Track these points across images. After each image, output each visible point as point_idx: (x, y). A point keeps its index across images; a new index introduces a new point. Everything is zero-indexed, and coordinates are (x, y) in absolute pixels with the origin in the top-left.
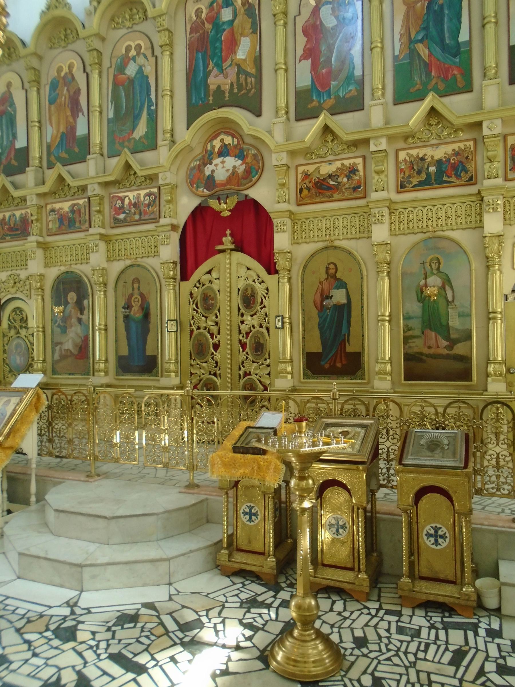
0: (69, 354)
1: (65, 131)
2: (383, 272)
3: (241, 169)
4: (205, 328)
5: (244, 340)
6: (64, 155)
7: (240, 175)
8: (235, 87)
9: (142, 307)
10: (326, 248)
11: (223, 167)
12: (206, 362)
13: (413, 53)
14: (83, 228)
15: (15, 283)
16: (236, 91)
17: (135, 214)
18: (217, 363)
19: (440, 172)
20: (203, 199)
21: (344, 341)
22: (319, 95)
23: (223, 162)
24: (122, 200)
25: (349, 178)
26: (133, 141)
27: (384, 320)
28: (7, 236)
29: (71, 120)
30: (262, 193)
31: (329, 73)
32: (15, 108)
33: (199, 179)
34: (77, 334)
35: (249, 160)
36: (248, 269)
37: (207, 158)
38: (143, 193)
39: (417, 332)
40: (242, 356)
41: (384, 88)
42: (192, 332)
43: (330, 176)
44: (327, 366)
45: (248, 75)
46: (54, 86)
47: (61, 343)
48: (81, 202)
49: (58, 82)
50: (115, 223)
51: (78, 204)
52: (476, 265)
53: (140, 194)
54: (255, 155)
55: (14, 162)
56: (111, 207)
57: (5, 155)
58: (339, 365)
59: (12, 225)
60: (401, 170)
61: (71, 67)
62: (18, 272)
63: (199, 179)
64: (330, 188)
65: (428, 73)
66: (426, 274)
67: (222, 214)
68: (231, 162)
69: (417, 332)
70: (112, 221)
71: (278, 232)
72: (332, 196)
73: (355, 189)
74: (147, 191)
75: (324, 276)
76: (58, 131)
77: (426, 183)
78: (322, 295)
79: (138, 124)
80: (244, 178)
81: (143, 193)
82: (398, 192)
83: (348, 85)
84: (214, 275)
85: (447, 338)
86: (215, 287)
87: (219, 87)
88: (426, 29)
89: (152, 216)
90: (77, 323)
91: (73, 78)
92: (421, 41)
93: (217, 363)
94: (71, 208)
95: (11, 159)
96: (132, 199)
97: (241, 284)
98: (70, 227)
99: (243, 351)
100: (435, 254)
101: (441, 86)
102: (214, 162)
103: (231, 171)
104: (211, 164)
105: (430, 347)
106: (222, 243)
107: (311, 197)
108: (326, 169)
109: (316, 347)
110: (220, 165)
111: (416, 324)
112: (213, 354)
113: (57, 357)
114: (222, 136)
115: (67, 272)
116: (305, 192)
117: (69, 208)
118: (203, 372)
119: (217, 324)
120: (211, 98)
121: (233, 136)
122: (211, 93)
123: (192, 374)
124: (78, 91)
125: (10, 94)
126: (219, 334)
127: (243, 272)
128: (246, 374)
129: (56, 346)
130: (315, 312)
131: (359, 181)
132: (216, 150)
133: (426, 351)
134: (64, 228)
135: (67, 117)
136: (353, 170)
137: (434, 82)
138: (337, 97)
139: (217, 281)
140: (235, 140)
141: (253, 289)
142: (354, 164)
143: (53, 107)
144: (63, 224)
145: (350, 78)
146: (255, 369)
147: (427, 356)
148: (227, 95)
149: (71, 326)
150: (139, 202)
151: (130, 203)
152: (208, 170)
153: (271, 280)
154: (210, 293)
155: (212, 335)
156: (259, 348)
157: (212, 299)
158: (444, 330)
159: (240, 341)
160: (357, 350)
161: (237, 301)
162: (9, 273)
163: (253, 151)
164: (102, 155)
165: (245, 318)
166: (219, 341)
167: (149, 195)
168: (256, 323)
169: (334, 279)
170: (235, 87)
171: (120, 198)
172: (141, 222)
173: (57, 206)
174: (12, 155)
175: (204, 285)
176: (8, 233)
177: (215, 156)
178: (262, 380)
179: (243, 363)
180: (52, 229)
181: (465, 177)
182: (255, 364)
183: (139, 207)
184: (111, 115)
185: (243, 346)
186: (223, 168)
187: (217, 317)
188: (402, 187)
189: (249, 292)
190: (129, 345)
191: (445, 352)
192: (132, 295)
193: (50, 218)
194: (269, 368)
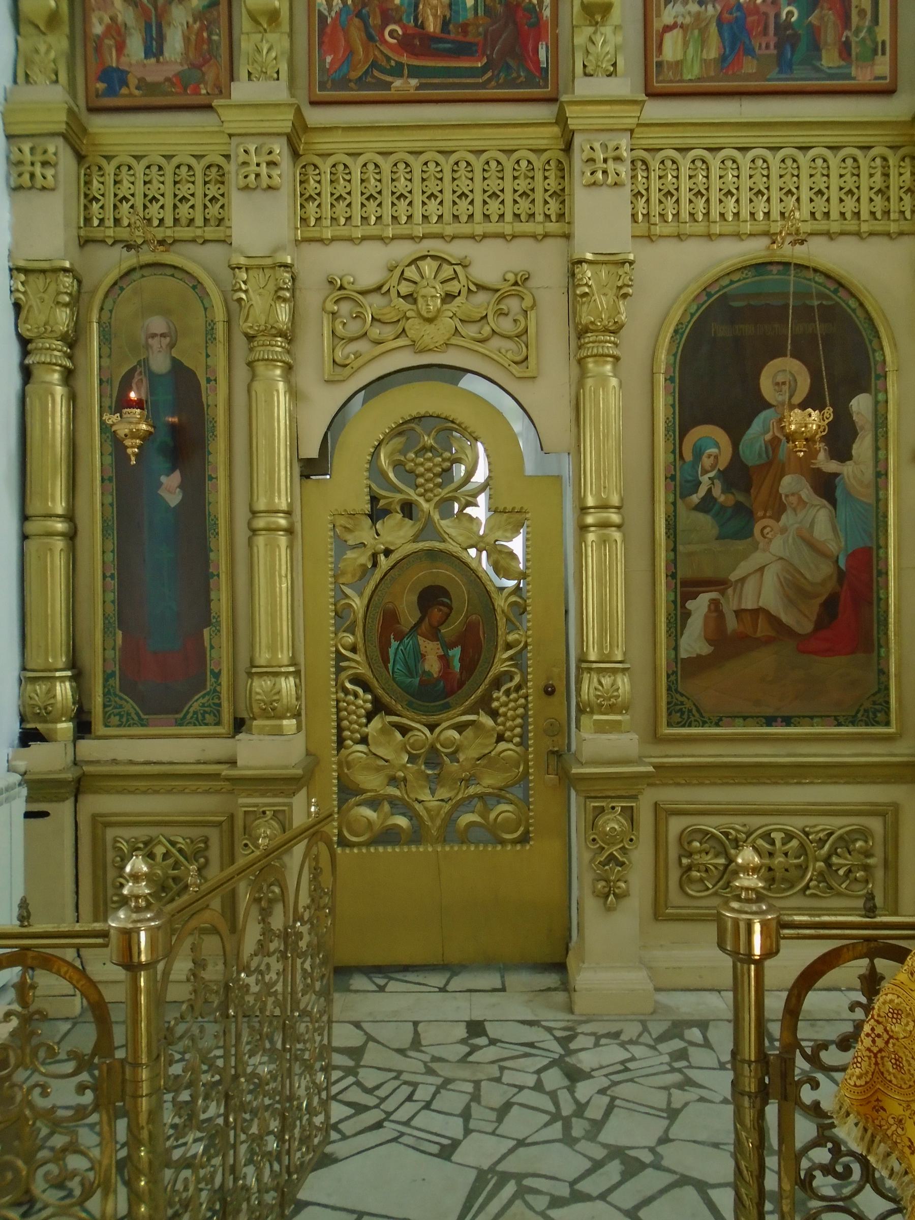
0: (763, 629)
14: (863, 76)
15: (449, 297)
28: (398, 71)
47: (719, 584)
59: (432, 26)
62: (455, 250)
90: (806, 492)
98: (783, 64)
113: (694, 642)
115: (760, 267)
129: (694, 596)
134: (749, 66)
144: (749, 51)
149: (778, 508)
162: (404, 251)
176: (404, 59)
180: (678, 65)
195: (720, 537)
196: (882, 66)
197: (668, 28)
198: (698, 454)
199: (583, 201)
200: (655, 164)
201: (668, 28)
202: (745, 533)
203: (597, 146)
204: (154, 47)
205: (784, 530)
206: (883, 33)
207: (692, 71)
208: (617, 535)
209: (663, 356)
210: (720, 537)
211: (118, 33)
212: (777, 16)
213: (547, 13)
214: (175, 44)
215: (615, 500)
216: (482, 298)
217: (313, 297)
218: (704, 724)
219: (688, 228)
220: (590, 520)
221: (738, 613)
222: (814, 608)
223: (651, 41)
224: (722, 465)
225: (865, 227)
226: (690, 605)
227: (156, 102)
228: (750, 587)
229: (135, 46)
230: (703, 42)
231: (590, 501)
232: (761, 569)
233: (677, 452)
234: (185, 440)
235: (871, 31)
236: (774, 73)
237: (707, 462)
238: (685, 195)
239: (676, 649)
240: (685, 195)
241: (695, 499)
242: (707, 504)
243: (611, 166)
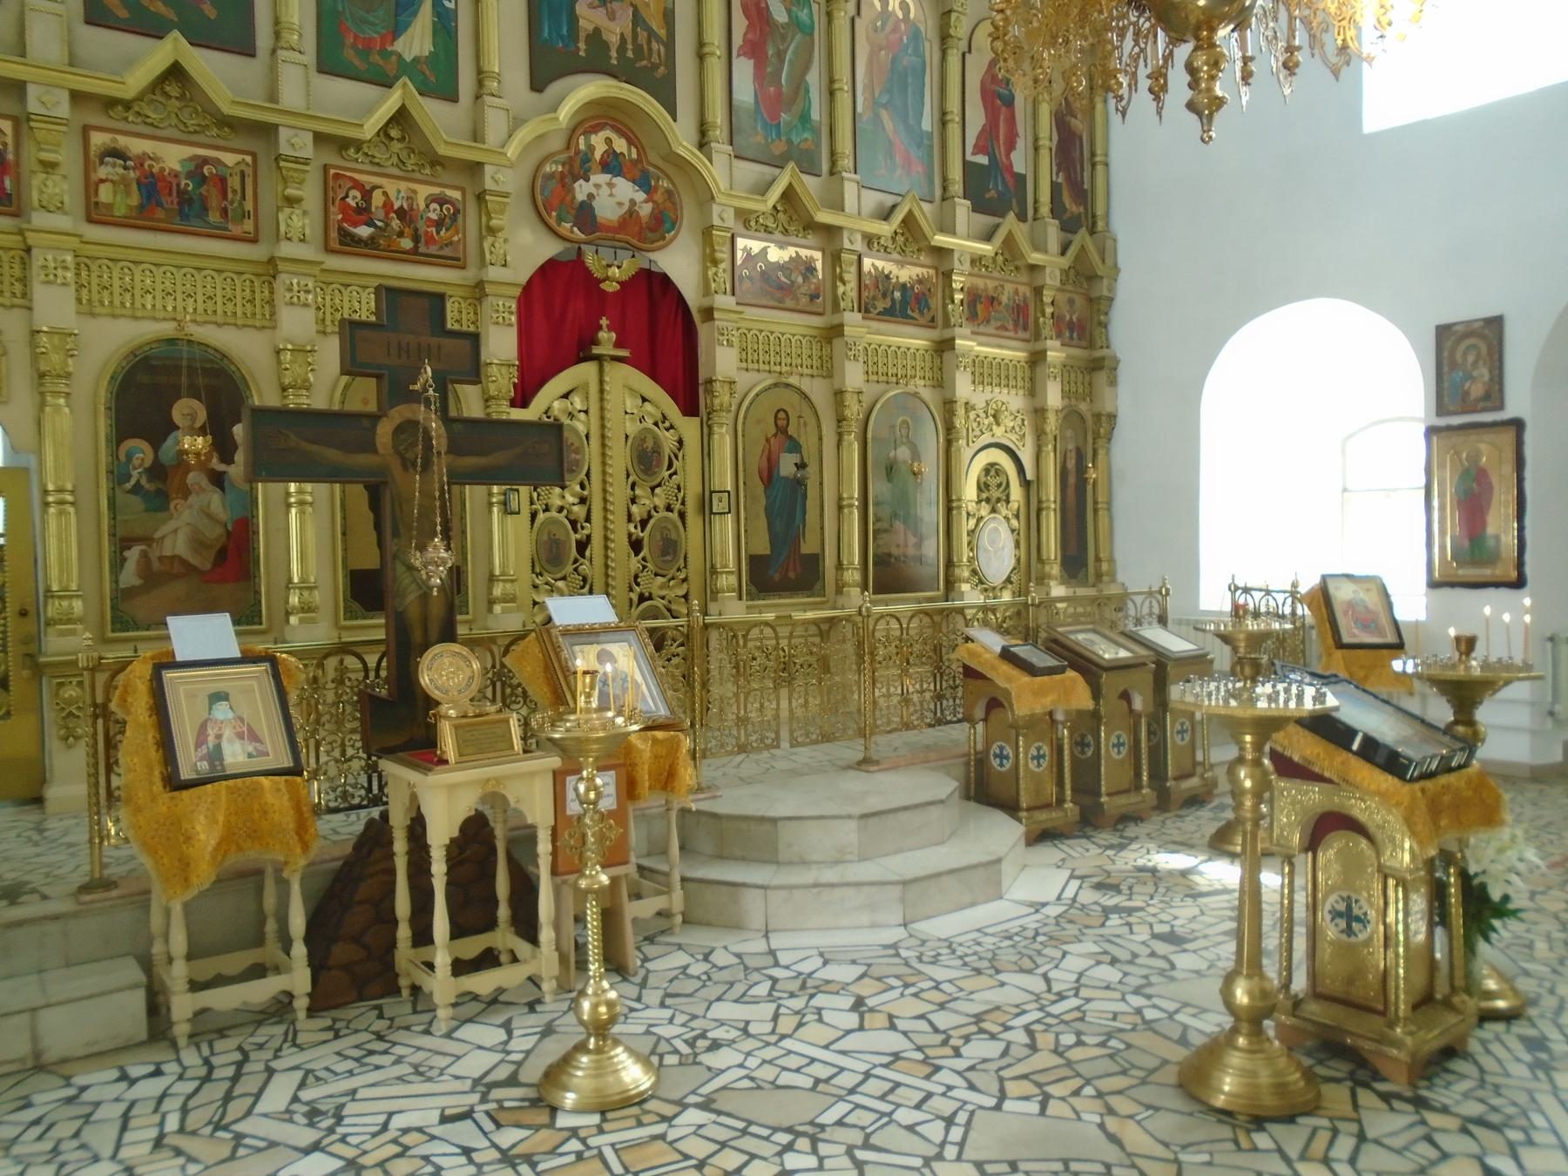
2: (850, 433)
3: (645, 210)
4: (561, 509)
5: (638, 533)
7: (644, 220)
8: (630, 46)
11: (611, 195)
12: (564, 578)
14: (236, 230)
16: (630, 54)
17: (401, 234)
18: (585, 580)
19: (904, 302)
20: (568, 245)
24: (367, 195)
25: (805, 278)
26: (394, 58)
27: (851, 506)
30: (678, 262)
31: (779, 93)
33: (553, 198)
34: (210, 516)
35: (659, 197)
36: (644, 400)
37: (579, 166)
38: (424, 191)
39: (885, 525)
40: (635, 563)
42: (534, 516)
44: (777, 577)
45: (652, 34)
48: (230, 159)
50: (341, 243)
51: (218, 162)
53: (415, 192)
54: (669, 193)
58: (792, 575)
63: (562, 201)
67: (603, 286)
68: (625, 190)
70: (334, 234)
74: (436, 190)
75: (773, 430)
77: (890, 314)
79: (407, 26)
81: (424, 191)
84: (577, 402)
86: (581, 428)
87: (597, 31)
89: (447, 252)
90: (205, 482)
92: (885, 106)
94: (192, 166)
96: (393, 197)
97: (632, 428)
98: (184, 216)
99: (636, 554)
103: (626, 208)
104: (587, 180)
106: (596, 342)
109: (762, 546)
110: (605, 190)
113: (129, 576)
114: (607, 133)
115: (171, 341)
117: (183, 162)
119: (583, 501)
120: (582, 45)
121: (630, 142)
122: (582, 35)
123: (535, 603)
126: (588, 519)
127: (631, 404)
128: (642, 598)
130: (760, 488)
134: (160, 214)
137: (899, 171)
140: (634, 150)
142: (812, 259)
144: (159, 204)
145: (805, 117)
146: (662, 587)
148: (614, 54)
149: (186, 493)
150: (412, 209)
151: (388, 205)
152: (581, 190)
153: (689, 428)
155: (574, 523)
156: (670, 548)
159: (630, 535)
160: (816, 550)
161: (620, 458)
163: (665, 184)
165: (638, 492)
166: (589, 537)
167: (441, 201)
168: (660, 501)
170: (630, 46)
171: (358, 185)
172: (414, 256)
173: (137, 146)
178: (673, 607)
179: (636, 577)
180: (109, 206)
182: (660, 580)
183: (411, 221)
185: (636, 546)
186: (613, 196)
187: (583, 487)
189: (649, 444)
193: (103, 172)
194: (685, 585)
195: (147, 510)
196: (248, 225)
197: (102, 181)
198: (129, 457)
199: (39, 292)
200: (94, 267)
201: (102, 181)
202: (164, 507)
203: (50, 257)
205: (190, 507)
206: (249, 206)
207: (120, 211)
208: (71, 510)
209: (102, 393)
210: (147, 510)
212: (178, 185)
213: (10, 157)
215: (69, 486)
218: (138, 629)
219: (118, 311)
220: (50, 499)
221: (161, 559)
222: (211, 555)
223: (91, 187)
224: (148, 463)
225: (239, 322)
226: (126, 554)
228: (168, 543)
230: (128, 193)
231: (51, 487)
232: (175, 531)
233: (114, 455)
235: (241, 204)
236: (177, 220)
237: (136, 462)
238: (117, 290)
239: (117, 582)
240: (117, 290)
241: (128, 486)
242: (137, 489)
243: (60, 272)
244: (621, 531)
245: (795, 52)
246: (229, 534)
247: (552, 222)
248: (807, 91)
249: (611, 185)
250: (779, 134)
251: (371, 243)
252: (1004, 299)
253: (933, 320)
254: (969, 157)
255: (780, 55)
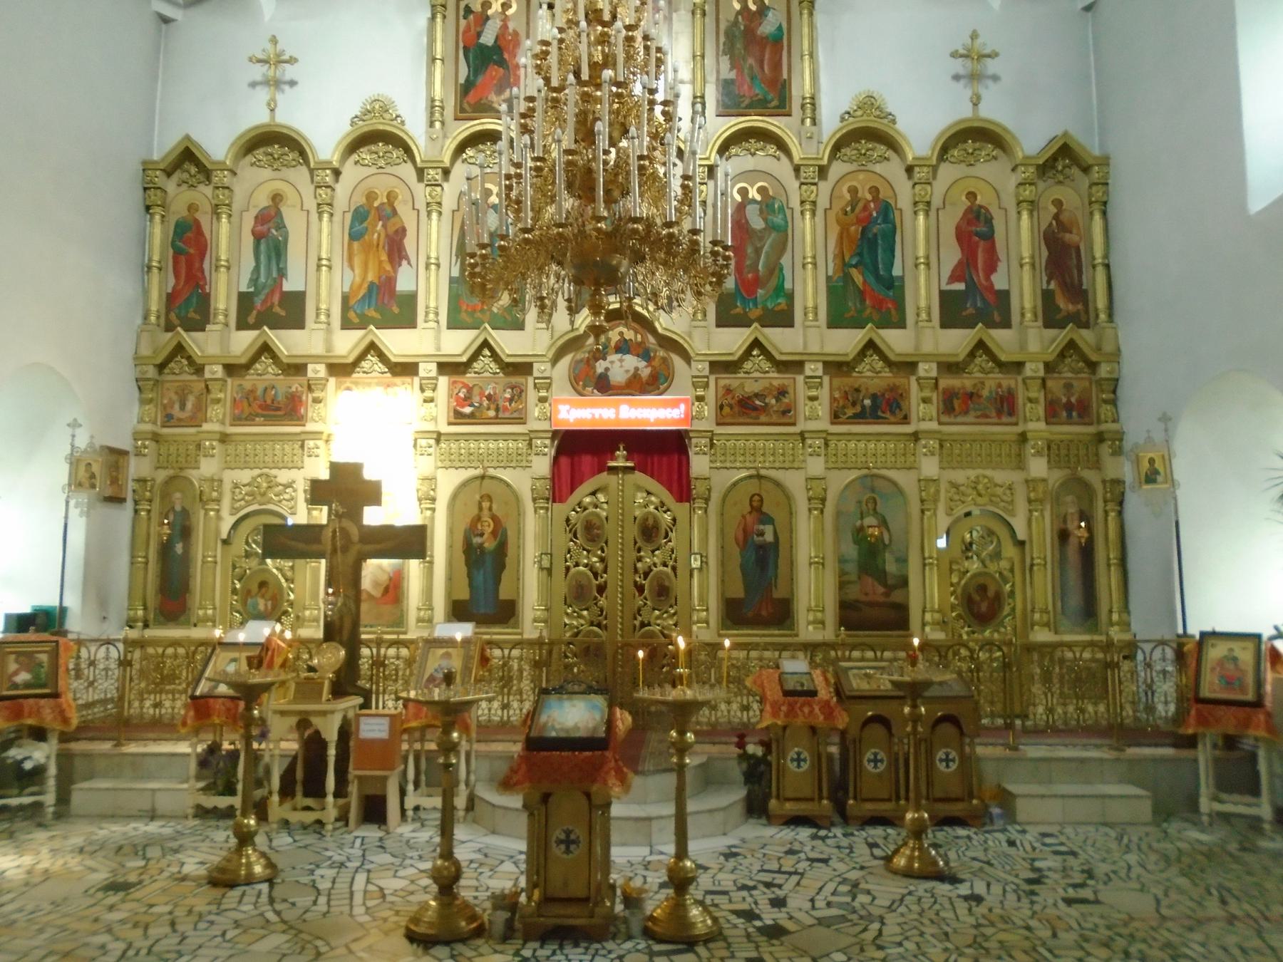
1: (376, 281)
3: (645, 373)
4: (586, 566)
6: (372, 313)
9: (494, 533)
10: (750, 477)
13: (847, 278)
17: (488, 409)
19: (875, 407)
21: (770, 584)
22: (744, 300)
23: (621, 360)
24: (470, 390)
25: (778, 400)
28: (257, 415)
29: (388, 267)
32: (287, 233)
35: (656, 363)
36: (649, 493)
41: (816, 308)
42: (568, 569)
43: (757, 395)
44: (750, 614)
46: (360, 215)
49: (368, 212)
52: (915, 508)
55: (277, 309)
56: (450, 396)
57: (262, 297)
58: (764, 613)
59: (269, 402)
60: (835, 399)
61: (391, 196)
64: (756, 408)
65: (863, 301)
66: (862, 514)
68: (632, 361)
69: (854, 577)
70: (452, 414)
71: (697, 453)
72: (758, 418)
73: (785, 412)
75: (749, 509)
76: (364, 279)
77: (861, 417)
78: (745, 531)
80: (648, 384)
82: (832, 423)
83: (778, 297)
84: (601, 498)
85: (885, 585)
88: (860, 254)
89: (515, 415)
91: (395, 212)
92: (855, 266)
93: (602, 611)
95: (272, 306)
99: (640, 595)
100: (873, 493)
101: (876, 316)
102: (610, 358)
104: (605, 359)
105: (866, 594)
107: (733, 416)
108: (751, 387)
109: (738, 591)
110: (618, 364)
111: (852, 568)
112: (596, 598)
114: (621, 329)
116: (727, 410)
118: (582, 621)
119: (602, 560)
124: (402, 231)
125: (278, 213)
126: (605, 572)
128: (643, 625)
130: (736, 551)
131: (788, 405)
132: (613, 344)
133: (863, 598)
135: (380, 262)
136: (782, 392)
137: (868, 311)
138: (765, 308)
139: (605, 506)
140: (639, 337)
141: (656, 521)
143: (356, 245)
145: (779, 290)
146: (658, 618)
147: (863, 603)
152: (600, 366)
153: (681, 509)
154: (595, 521)
155: (596, 575)
156: (663, 592)
157: (598, 528)
158: (881, 576)
159: (635, 582)
160: (787, 596)
161: (633, 531)
162: (257, 472)
164: (437, 322)
169: (758, 510)
171: (465, 386)
172: (496, 420)
174: (276, 299)
175: (585, 509)
176: (260, 411)
177: (610, 350)
179: (639, 610)
181: (900, 415)
182: (657, 612)
184: (456, 273)
185: (640, 589)
188: (836, 417)
189: (651, 522)
190: (471, 585)
191: (882, 599)
192: (478, 519)
204: (183, 407)
211: (172, 403)
214: (189, 405)
216: (281, 488)
217: (227, 487)
222: (381, 589)
227: (181, 423)
229: (177, 406)
234: (185, 532)
244: (630, 577)
245: (771, 246)
246: (391, 579)
247: (580, 388)
248: (781, 269)
249: (621, 360)
250: (756, 305)
251: (472, 415)
252: (985, 393)
253: (906, 417)
254: (945, 287)
255: (758, 252)
